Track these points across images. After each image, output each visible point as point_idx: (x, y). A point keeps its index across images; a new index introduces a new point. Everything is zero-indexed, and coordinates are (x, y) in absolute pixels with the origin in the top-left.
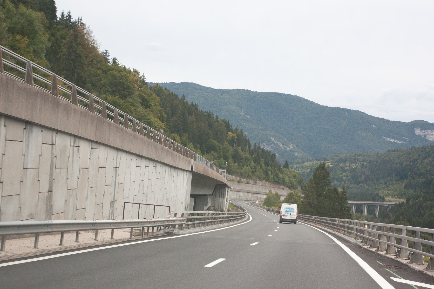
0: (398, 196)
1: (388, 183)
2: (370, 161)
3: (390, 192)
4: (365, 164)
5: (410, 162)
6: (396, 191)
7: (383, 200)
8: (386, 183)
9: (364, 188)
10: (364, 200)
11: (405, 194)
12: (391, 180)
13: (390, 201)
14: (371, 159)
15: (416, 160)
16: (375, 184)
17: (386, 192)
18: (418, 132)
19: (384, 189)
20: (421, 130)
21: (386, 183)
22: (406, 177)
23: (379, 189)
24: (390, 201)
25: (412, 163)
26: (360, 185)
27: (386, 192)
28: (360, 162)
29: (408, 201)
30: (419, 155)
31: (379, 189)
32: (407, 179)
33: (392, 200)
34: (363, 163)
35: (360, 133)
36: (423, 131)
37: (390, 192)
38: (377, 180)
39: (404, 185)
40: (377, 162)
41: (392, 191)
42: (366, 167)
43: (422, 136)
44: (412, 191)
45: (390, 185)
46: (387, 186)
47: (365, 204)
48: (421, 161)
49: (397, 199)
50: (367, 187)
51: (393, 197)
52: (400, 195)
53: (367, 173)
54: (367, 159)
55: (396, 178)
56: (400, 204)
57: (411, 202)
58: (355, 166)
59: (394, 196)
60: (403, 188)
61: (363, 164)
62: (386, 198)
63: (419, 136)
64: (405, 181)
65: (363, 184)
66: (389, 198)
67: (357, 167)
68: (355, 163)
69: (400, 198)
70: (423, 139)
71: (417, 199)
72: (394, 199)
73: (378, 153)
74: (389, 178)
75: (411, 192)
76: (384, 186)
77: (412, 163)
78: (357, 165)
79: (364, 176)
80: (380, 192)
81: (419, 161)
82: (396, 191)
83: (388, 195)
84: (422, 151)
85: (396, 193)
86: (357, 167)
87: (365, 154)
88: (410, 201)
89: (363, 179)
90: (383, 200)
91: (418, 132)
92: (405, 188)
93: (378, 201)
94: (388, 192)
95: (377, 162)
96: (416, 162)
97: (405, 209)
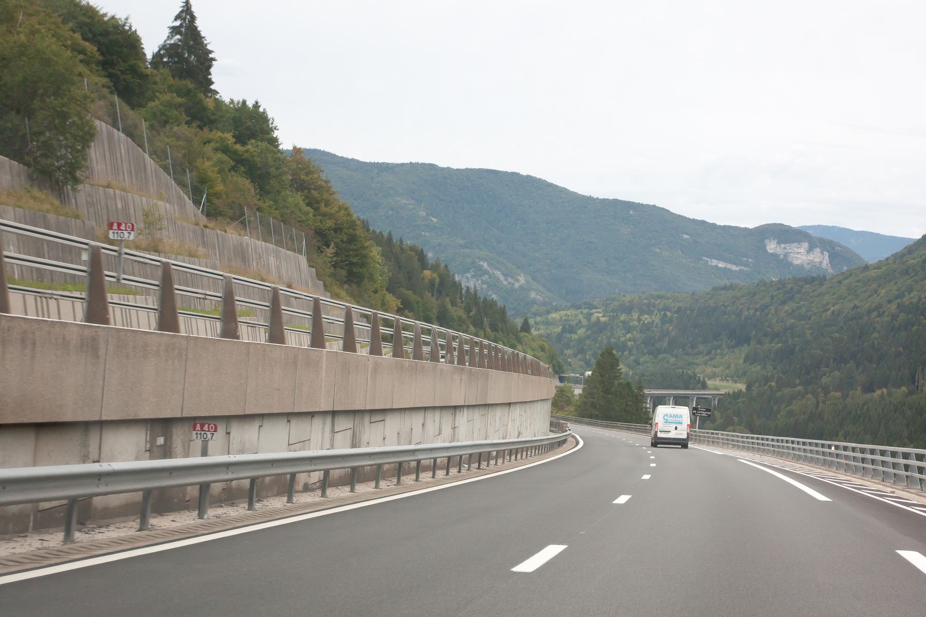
0: (732, 377)
1: (713, 352)
2: (680, 308)
3: (717, 370)
4: (669, 314)
5: (756, 310)
6: (728, 367)
7: (704, 386)
8: (709, 353)
9: (668, 362)
10: (668, 388)
11: (744, 374)
12: (719, 347)
13: (716, 389)
14: (680, 304)
15: (767, 307)
16: (688, 354)
17: (709, 370)
18: (772, 247)
19: (706, 364)
20: (778, 243)
21: (709, 353)
22: (747, 340)
23: (697, 364)
24: (716, 389)
25: (758, 313)
26: (661, 356)
27: (709, 370)
28: (659, 311)
29: (749, 387)
30: (772, 297)
31: (697, 364)
32: (749, 345)
33: (721, 386)
34: (665, 314)
35: (658, 250)
36: (783, 246)
37: (717, 370)
38: (693, 347)
39: (743, 356)
40: (692, 311)
41: (721, 368)
42: (671, 321)
43: (779, 256)
44: (759, 367)
45: (718, 357)
46: (711, 359)
47: (670, 395)
48: (776, 309)
49: (730, 384)
50: (673, 360)
51: (722, 380)
52: (737, 376)
53: (673, 333)
54: (673, 304)
55: (729, 342)
56: (734, 393)
57: (755, 390)
58: (649, 320)
59: (725, 378)
60: (741, 361)
61: (665, 315)
62: (709, 383)
63: (775, 255)
64: (745, 349)
65: (664, 355)
66: (717, 382)
67: (653, 322)
68: (650, 313)
69: (736, 382)
70: (782, 262)
71: (765, 385)
72: (725, 383)
73: (693, 294)
74: (716, 343)
75: (756, 369)
76: (707, 358)
77: (758, 313)
78: (653, 317)
79: (666, 340)
80: (698, 370)
81: (772, 309)
82: (728, 367)
83: (713, 376)
84: (779, 289)
85: (727, 371)
86: (653, 322)
87: (669, 295)
88: (753, 388)
89: (665, 345)
90: (704, 386)
91: (772, 247)
92: (745, 362)
93: (694, 389)
94: (714, 369)
95: (692, 311)
96: (766, 311)
97: (743, 402)
